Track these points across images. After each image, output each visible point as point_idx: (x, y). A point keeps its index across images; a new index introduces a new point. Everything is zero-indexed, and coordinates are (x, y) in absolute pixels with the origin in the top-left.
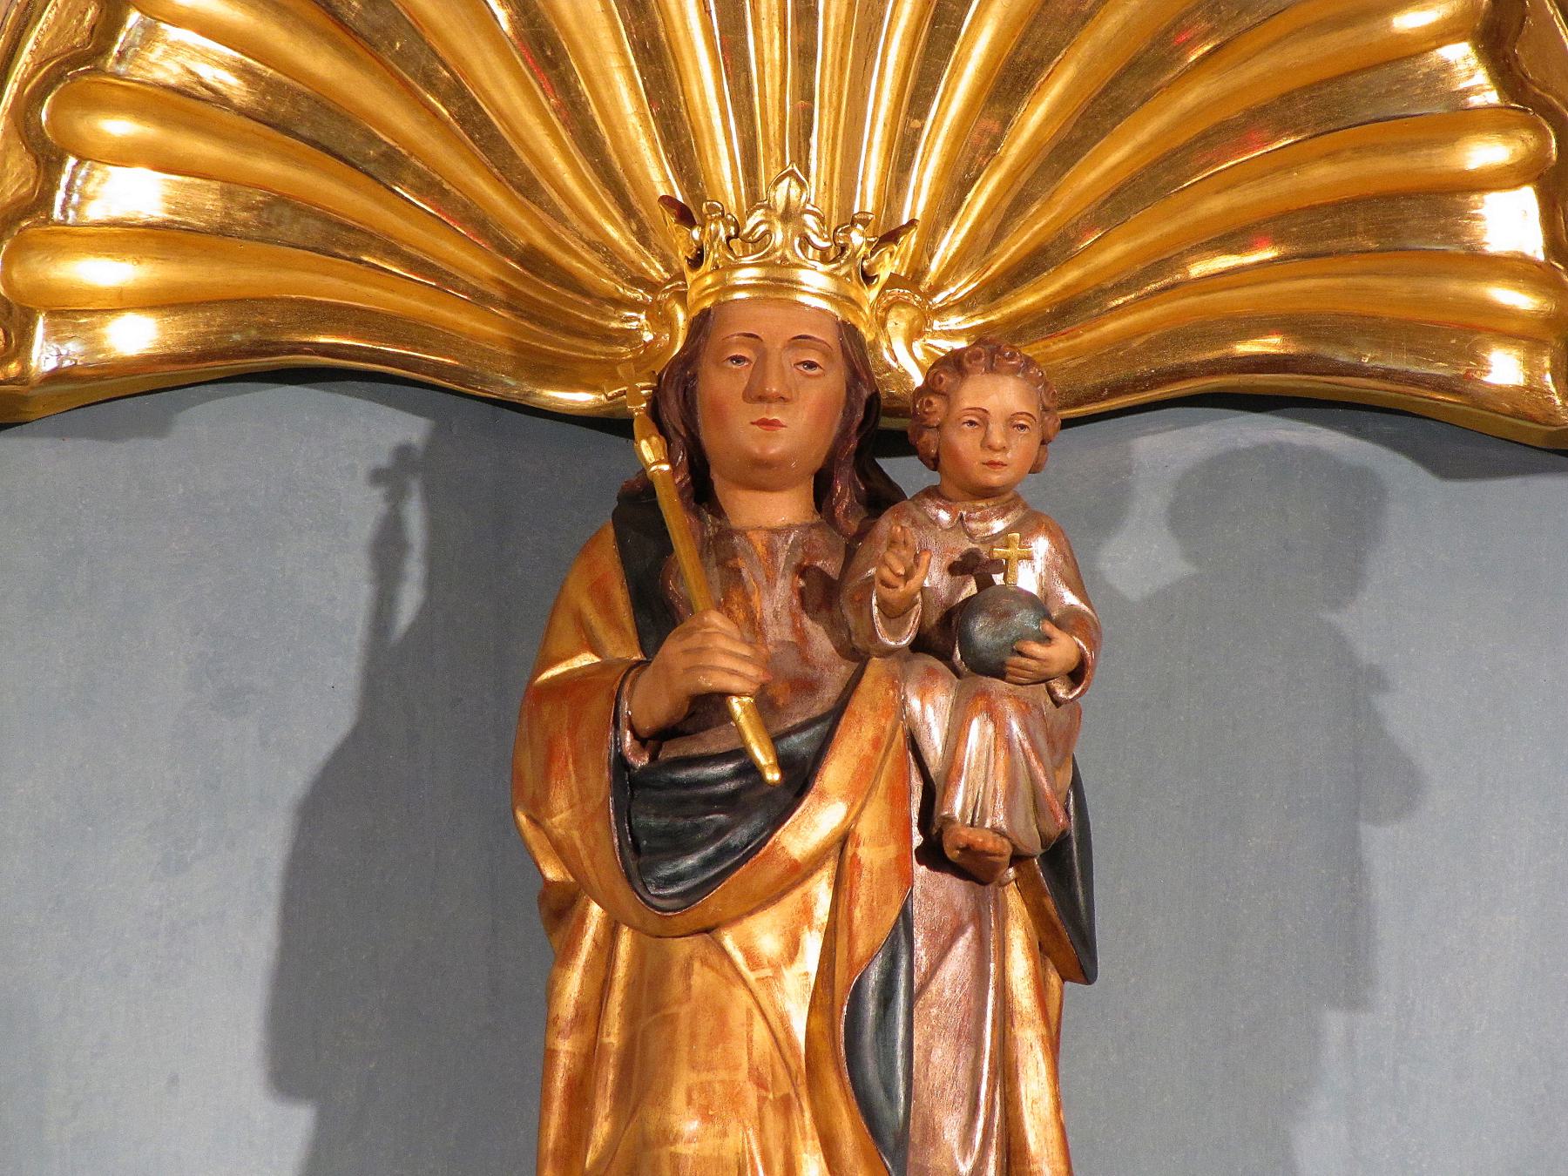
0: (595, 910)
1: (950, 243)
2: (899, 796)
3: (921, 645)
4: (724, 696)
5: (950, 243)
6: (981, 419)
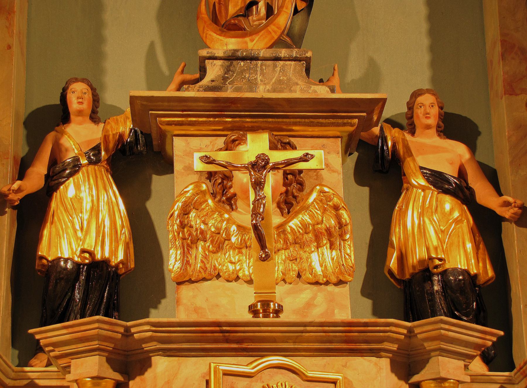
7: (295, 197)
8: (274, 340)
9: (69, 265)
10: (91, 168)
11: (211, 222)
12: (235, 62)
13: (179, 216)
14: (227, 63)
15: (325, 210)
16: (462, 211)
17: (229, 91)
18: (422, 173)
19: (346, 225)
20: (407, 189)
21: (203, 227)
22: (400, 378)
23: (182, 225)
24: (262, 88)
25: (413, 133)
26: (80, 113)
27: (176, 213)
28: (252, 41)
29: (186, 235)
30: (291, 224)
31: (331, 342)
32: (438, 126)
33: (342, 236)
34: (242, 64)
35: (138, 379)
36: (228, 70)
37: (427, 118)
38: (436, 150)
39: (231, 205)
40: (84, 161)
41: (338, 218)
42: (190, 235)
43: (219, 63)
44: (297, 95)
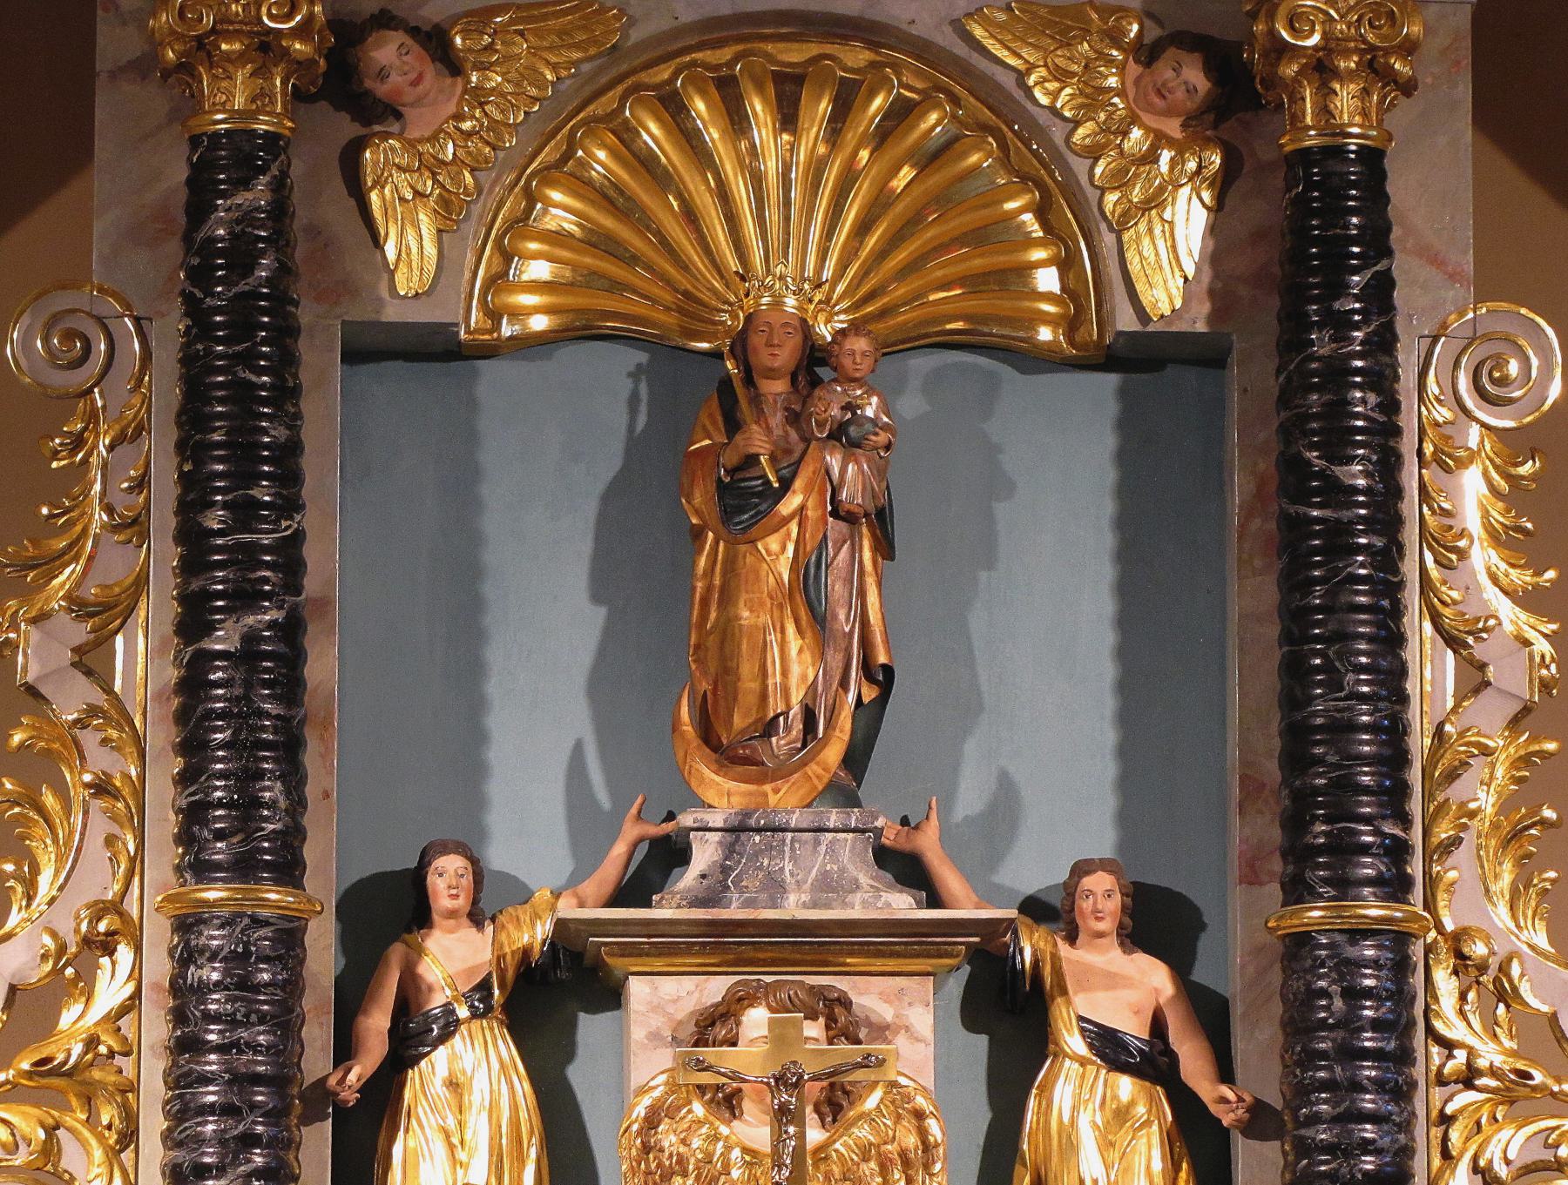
0: (710, 534)
1: (840, 288)
2: (822, 493)
4: (758, 455)
5: (840, 288)
6: (853, 353)
7: (847, 1093)
11: (696, 1143)
12: (743, 836)
13: (639, 1133)
14: (730, 837)
15: (899, 1117)
16: (1152, 1100)
17: (734, 905)
18: (1083, 1030)
19: (937, 1145)
20: (1056, 1056)
21: (682, 1149)
23: (646, 1149)
24: (792, 898)
25: (1072, 939)
26: (452, 914)
27: (635, 1127)
28: (776, 791)
29: (653, 1166)
30: (838, 1146)
32: (1121, 926)
33: (927, 1167)
34: (757, 838)
36: (730, 850)
37: (1098, 919)
38: (1112, 981)
39: (732, 1109)
41: (923, 1133)
42: (658, 1166)
43: (715, 837)
44: (856, 913)
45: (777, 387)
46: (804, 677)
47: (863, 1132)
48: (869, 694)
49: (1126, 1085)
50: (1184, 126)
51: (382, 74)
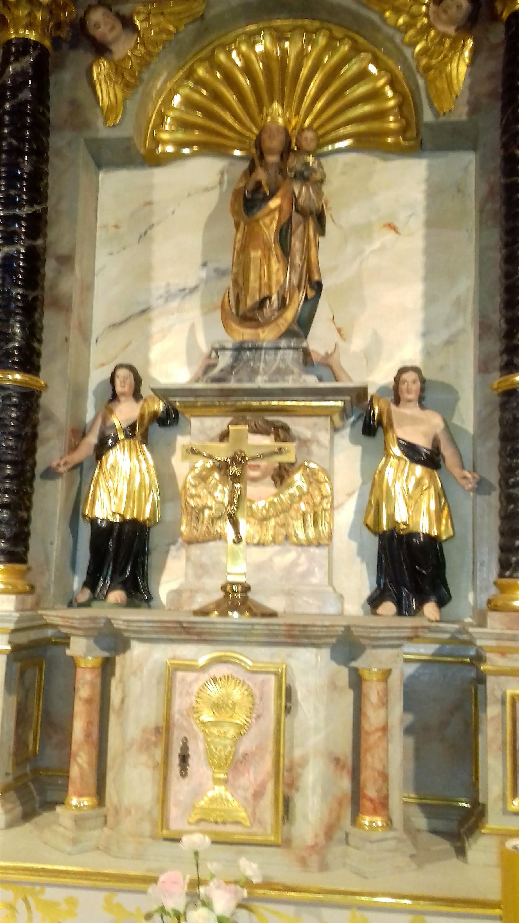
3: (295, 176)
8: (228, 634)
9: (104, 525)
10: (126, 442)
22: (339, 663)
31: (276, 636)
35: (122, 656)
36: (236, 359)
40: (121, 436)
45: (273, 159)
46: (278, 282)
47: (293, 490)
48: (311, 294)
49: (419, 469)
50: (457, 30)
51: (97, 25)
